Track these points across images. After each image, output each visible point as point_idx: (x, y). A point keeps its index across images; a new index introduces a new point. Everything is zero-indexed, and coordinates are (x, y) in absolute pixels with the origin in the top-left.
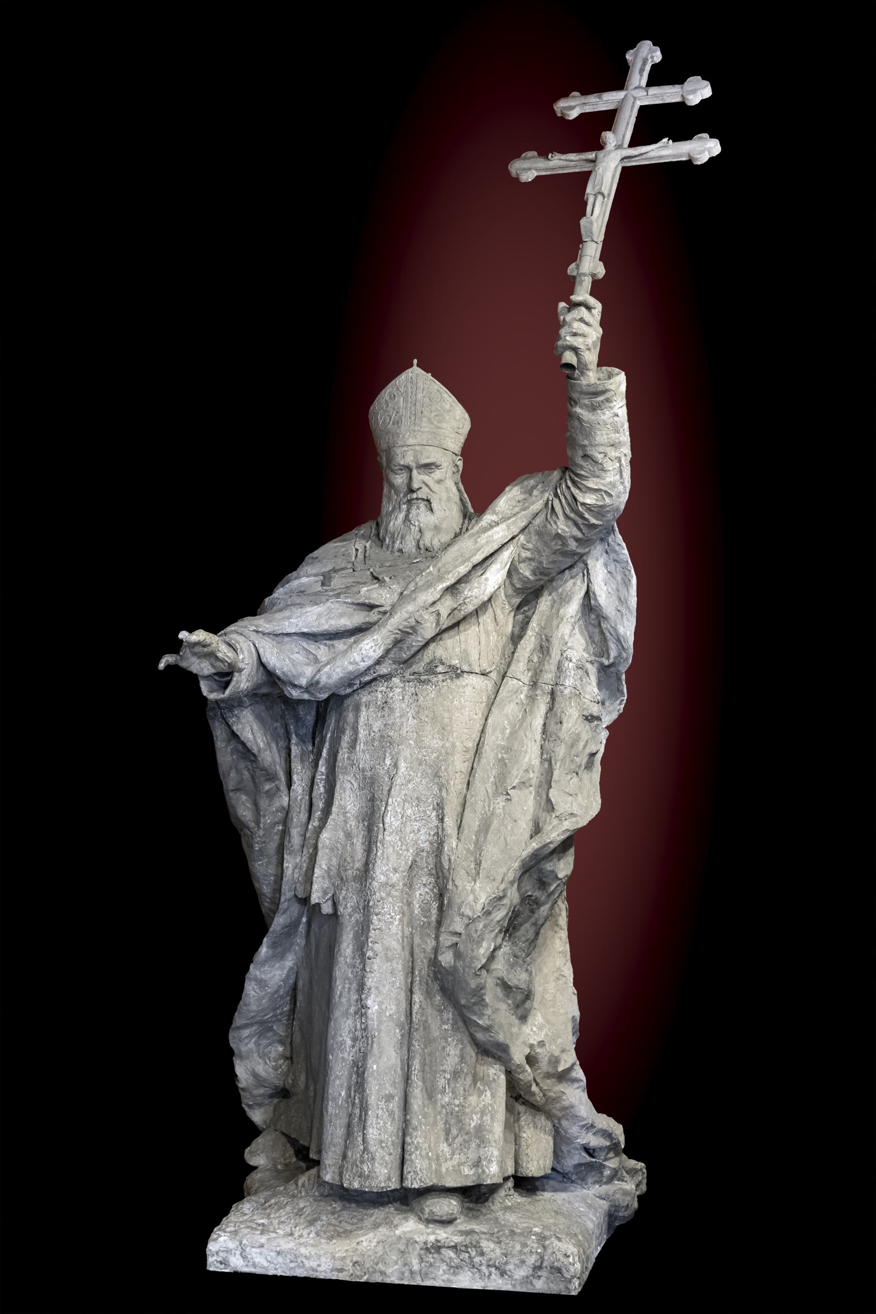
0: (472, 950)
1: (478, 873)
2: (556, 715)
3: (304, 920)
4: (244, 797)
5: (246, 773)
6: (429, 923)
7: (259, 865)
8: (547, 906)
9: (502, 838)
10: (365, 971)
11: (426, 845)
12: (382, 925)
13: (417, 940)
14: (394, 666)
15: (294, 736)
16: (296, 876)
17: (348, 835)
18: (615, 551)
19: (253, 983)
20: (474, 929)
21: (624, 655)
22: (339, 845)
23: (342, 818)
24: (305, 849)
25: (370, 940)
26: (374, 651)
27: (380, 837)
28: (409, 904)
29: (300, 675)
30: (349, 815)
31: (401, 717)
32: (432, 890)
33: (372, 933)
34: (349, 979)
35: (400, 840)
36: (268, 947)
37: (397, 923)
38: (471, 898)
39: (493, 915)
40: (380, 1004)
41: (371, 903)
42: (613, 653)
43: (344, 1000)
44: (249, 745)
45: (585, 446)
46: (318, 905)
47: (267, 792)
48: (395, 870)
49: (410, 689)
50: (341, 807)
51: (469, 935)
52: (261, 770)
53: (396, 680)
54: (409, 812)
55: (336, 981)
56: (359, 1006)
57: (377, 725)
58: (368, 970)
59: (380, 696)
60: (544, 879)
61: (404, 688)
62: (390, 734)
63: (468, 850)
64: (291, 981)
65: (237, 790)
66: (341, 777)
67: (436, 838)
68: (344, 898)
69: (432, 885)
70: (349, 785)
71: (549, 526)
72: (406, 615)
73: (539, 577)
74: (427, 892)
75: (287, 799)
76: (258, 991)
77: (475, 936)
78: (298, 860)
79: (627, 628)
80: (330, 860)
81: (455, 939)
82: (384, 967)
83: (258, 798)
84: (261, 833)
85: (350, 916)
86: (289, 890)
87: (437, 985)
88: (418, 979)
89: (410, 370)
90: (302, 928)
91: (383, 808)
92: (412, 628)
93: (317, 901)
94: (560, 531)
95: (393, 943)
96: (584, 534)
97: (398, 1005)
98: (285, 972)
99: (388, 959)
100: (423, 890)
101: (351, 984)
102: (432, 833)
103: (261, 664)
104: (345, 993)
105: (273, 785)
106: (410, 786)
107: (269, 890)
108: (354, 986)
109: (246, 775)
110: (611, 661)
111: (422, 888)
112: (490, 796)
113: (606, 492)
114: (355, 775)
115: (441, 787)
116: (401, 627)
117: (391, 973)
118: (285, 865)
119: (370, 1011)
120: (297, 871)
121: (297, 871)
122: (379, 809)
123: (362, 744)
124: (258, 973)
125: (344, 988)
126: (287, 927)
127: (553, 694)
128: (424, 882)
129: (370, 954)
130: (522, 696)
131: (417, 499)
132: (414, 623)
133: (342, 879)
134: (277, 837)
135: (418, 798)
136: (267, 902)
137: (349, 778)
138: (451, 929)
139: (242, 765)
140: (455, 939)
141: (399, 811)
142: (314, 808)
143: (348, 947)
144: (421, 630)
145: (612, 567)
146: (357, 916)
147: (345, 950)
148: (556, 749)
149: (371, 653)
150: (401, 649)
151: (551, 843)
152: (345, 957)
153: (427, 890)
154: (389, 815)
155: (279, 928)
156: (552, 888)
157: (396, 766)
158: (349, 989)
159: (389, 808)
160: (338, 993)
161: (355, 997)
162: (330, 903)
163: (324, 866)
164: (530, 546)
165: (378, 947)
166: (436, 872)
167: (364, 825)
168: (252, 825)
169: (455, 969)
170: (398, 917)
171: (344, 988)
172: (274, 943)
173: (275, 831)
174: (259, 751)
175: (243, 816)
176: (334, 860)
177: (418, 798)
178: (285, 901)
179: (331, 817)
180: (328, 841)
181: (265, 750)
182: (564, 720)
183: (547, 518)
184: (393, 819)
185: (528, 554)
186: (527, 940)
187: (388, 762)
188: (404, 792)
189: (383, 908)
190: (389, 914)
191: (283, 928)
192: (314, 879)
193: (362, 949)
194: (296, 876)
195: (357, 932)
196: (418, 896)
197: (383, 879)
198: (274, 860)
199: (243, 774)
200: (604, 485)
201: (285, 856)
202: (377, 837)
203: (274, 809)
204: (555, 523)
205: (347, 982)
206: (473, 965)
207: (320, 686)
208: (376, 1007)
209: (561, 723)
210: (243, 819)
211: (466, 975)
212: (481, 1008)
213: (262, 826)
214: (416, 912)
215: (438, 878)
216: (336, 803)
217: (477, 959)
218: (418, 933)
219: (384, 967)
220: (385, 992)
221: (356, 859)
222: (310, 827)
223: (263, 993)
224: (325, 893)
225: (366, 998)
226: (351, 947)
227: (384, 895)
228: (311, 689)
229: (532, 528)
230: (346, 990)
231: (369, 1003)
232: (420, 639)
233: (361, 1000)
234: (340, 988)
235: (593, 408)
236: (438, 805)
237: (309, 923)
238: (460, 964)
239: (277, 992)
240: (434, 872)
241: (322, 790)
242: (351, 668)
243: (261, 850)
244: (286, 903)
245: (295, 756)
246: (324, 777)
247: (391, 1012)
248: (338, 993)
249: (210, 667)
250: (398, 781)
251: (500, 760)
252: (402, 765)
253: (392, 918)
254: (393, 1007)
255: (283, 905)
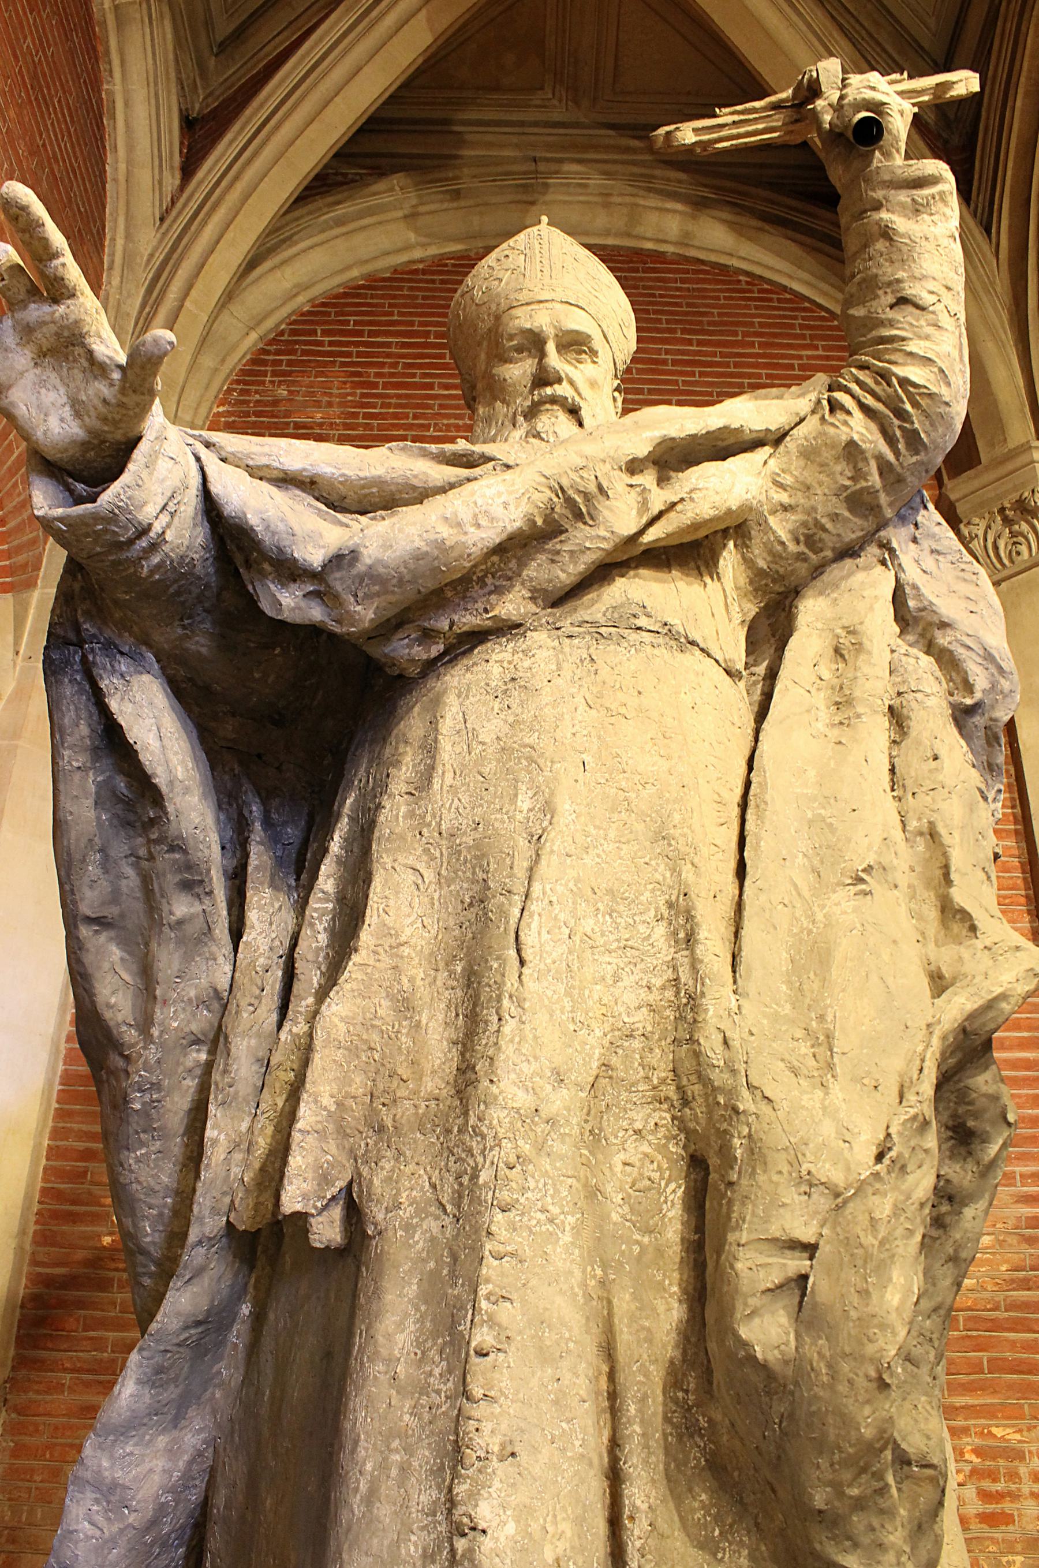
0: (864, 1293)
1: (831, 1066)
2: (919, 743)
3: (245, 1309)
4: (116, 953)
5: (130, 872)
6: (659, 1251)
7: (138, 1160)
8: (982, 1204)
9: (874, 978)
10: (467, 1395)
11: (641, 1020)
12: (520, 1242)
13: (623, 1302)
14: (532, 608)
15: (258, 826)
16: (236, 1170)
17: (405, 1006)
18: (933, 536)
19: (90, 1495)
20: (863, 1219)
21: (1005, 685)
22: (375, 1037)
23: (387, 961)
24: (266, 1094)
25: (483, 1291)
26: (506, 505)
27: (511, 983)
28: (593, 1193)
29: (312, 537)
30: (406, 951)
31: (555, 704)
32: (662, 1149)
33: (490, 1268)
34: (403, 1434)
35: (568, 994)
36: (139, 1382)
37: (567, 1238)
38: (828, 1129)
39: (911, 1179)
40: (524, 1514)
41: (484, 1177)
42: (981, 681)
43: (384, 1511)
44: (145, 758)
45: (898, 281)
46: (301, 1218)
47: (180, 923)
48: (560, 1079)
49: (576, 649)
50: (386, 931)
51: (848, 1242)
52: (172, 849)
53: (539, 638)
54: (588, 925)
55: (356, 1442)
56: (443, 1528)
57: (490, 729)
58: (477, 1392)
59: (496, 670)
60: (971, 1123)
61: (559, 650)
62: (527, 741)
63: (775, 1018)
64: (194, 1497)
65: (100, 922)
66: (387, 859)
67: (669, 994)
68: (388, 1179)
69: (662, 1132)
70: (411, 877)
71: (832, 430)
72: (580, 462)
73: (802, 548)
74: (646, 1155)
75: (228, 968)
76: (100, 1519)
77: (869, 1240)
78: (244, 1126)
79: (997, 639)
80: (345, 1080)
81: (797, 1264)
82: (534, 1382)
83: (154, 945)
84: (152, 1054)
85: (409, 1228)
86: (215, 1211)
87: (695, 1452)
88: (637, 1428)
89: (533, 230)
90: (237, 1335)
91: (516, 912)
92: (587, 496)
93: (299, 1207)
94: (856, 437)
95: (559, 1300)
96: (897, 453)
97: (579, 1521)
98: (181, 1464)
99: (545, 1357)
100: (635, 1150)
101: (409, 1450)
102: (658, 982)
103: (210, 505)
104: (388, 1488)
105: (197, 908)
106: (588, 860)
107: (158, 1238)
108: (424, 1455)
109: (131, 879)
110: (978, 695)
111: (630, 1145)
112: (806, 893)
113: (941, 371)
114: (426, 851)
115: (674, 862)
116: (565, 483)
117: (556, 1402)
118: (210, 1133)
119: (487, 1543)
120: (238, 1156)
121: (238, 1156)
122: (504, 913)
123: (449, 775)
124: (105, 1464)
125: (383, 1466)
126: (198, 1323)
127: (897, 717)
128: (638, 1125)
129: (482, 1337)
130: (820, 725)
131: (554, 400)
132: (592, 488)
133: (381, 1129)
134: (191, 1084)
135: (610, 892)
136: (151, 1275)
137: (411, 861)
138: (775, 1230)
139: (119, 848)
140: (797, 1264)
141: (562, 917)
142: (297, 988)
143: (400, 1326)
144: (606, 513)
145: (929, 563)
146: (434, 1226)
147: (389, 1337)
148: (944, 806)
149: (498, 511)
150: (554, 558)
151: (1003, 997)
152: (391, 1361)
153: (645, 1148)
154: (534, 925)
155: (175, 1324)
156: (993, 1149)
157: (548, 809)
158: (404, 1469)
159: (534, 907)
160: (363, 1487)
161: (426, 1496)
162: (337, 1212)
163: (327, 1101)
164: (788, 480)
165: (505, 1313)
166: (680, 1088)
167: (451, 973)
168: (131, 1035)
169: (799, 1363)
170: (571, 1219)
171: (383, 1466)
172: (159, 1370)
173: (189, 1063)
174: (171, 783)
175: (109, 1006)
176: (358, 1079)
177: (610, 892)
178: (200, 1243)
179: (355, 958)
180: (342, 1027)
181: (187, 790)
182: (943, 753)
183: (823, 419)
184: (545, 936)
185: (784, 497)
186: (935, 1310)
187: (524, 802)
188: (572, 873)
189: (524, 1190)
190: (544, 1210)
191: (186, 1328)
192: (296, 1136)
193: (454, 1323)
194: (236, 1170)
195: (434, 1274)
196: (619, 1168)
197: (522, 1099)
198: (177, 1145)
199: (121, 876)
200: (938, 355)
201: (212, 1108)
202: (500, 985)
203: (193, 993)
204: (846, 423)
205: (395, 1444)
206: (870, 1349)
207: (360, 568)
208: (511, 1528)
209: (936, 758)
210: (108, 1015)
211: (842, 1388)
212: (876, 1523)
213: (155, 1032)
214: (615, 1217)
215: (685, 1102)
216: (372, 917)
217: (883, 1326)
218: (626, 1281)
219: (534, 1382)
220: (537, 1470)
221: (427, 1067)
222: (283, 1036)
223: (115, 1529)
224: (325, 1179)
225: (474, 1496)
226: (411, 1326)
227: (526, 1148)
228: (338, 582)
229: (789, 444)
230: (394, 1472)
231: (484, 1512)
232: (602, 533)
233: (451, 1503)
234: (369, 1467)
235: (916, 209)
236: (670, 905)
237: (258, 1318)
238: (816, 1349)
239: (154, 1523)
240: (671, 1091)
241: (323, 938)
242: (445, 532)
243: (145, 1113)
244: (202, 1251)
245: (257, 868)
246: (330, 906)
247: (562, 1546)
248: (363, 1487)
249: (67, 412)
250: (555, 843)
251: (810, 823)
252: (564, 806)
253: (551, 1221)
254: (566, 1527)
255: (194, 1256)
